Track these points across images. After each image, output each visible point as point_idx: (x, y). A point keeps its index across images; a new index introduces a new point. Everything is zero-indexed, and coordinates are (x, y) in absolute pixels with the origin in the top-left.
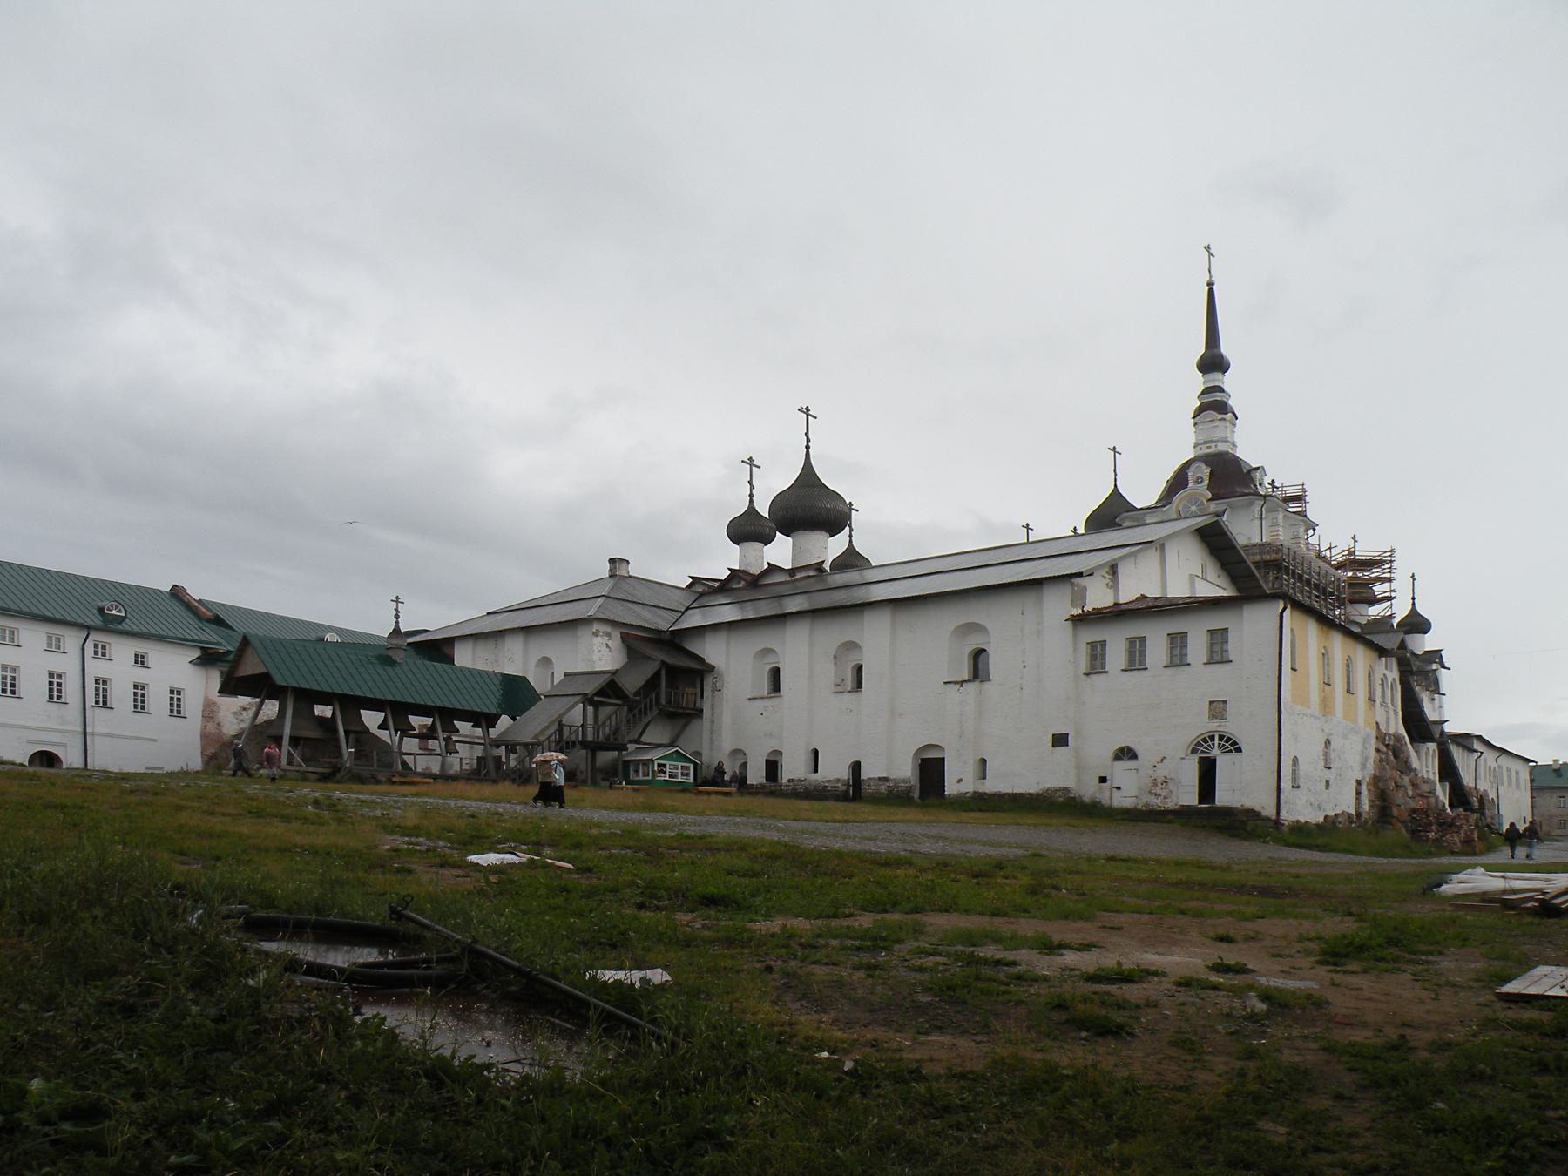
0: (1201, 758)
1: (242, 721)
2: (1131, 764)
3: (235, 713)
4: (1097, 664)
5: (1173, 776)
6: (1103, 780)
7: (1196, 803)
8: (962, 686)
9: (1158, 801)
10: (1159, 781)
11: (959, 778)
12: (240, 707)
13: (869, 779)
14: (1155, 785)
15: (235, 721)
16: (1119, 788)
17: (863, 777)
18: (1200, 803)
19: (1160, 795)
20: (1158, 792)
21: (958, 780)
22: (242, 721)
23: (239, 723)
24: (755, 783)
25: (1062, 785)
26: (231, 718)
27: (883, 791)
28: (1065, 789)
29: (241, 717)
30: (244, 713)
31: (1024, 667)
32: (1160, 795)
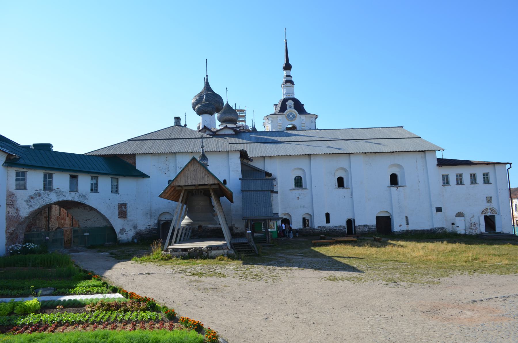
0: (484, 216)
1: (31, 206)
2: (462, 218)
3: (26, 201)
4: (446, 181)
5: (477, 222)
6: (453, 224)
7: (485, 231)
8: (398, 188)
9: (473, 231)
10: (473, 224)
11: (400, 224)
12: (30, 196)
13: (359, 226)
14: (471, 226)
15: (27, 207)
16: (458, 227)
17: (356, 225)
18: (486, 231)
19: (473, 229)
20: (473, 228)
21: (398, 225)
22: (31, 206)
23: (29, 208)
24: (296, 229)
25: (441, 226)
26: (24, 205)
27: (366, 231)
28: (443, 228)
29: (30, 204)
30: (32, 200)
31: (419, 182)
32: (473, 229)
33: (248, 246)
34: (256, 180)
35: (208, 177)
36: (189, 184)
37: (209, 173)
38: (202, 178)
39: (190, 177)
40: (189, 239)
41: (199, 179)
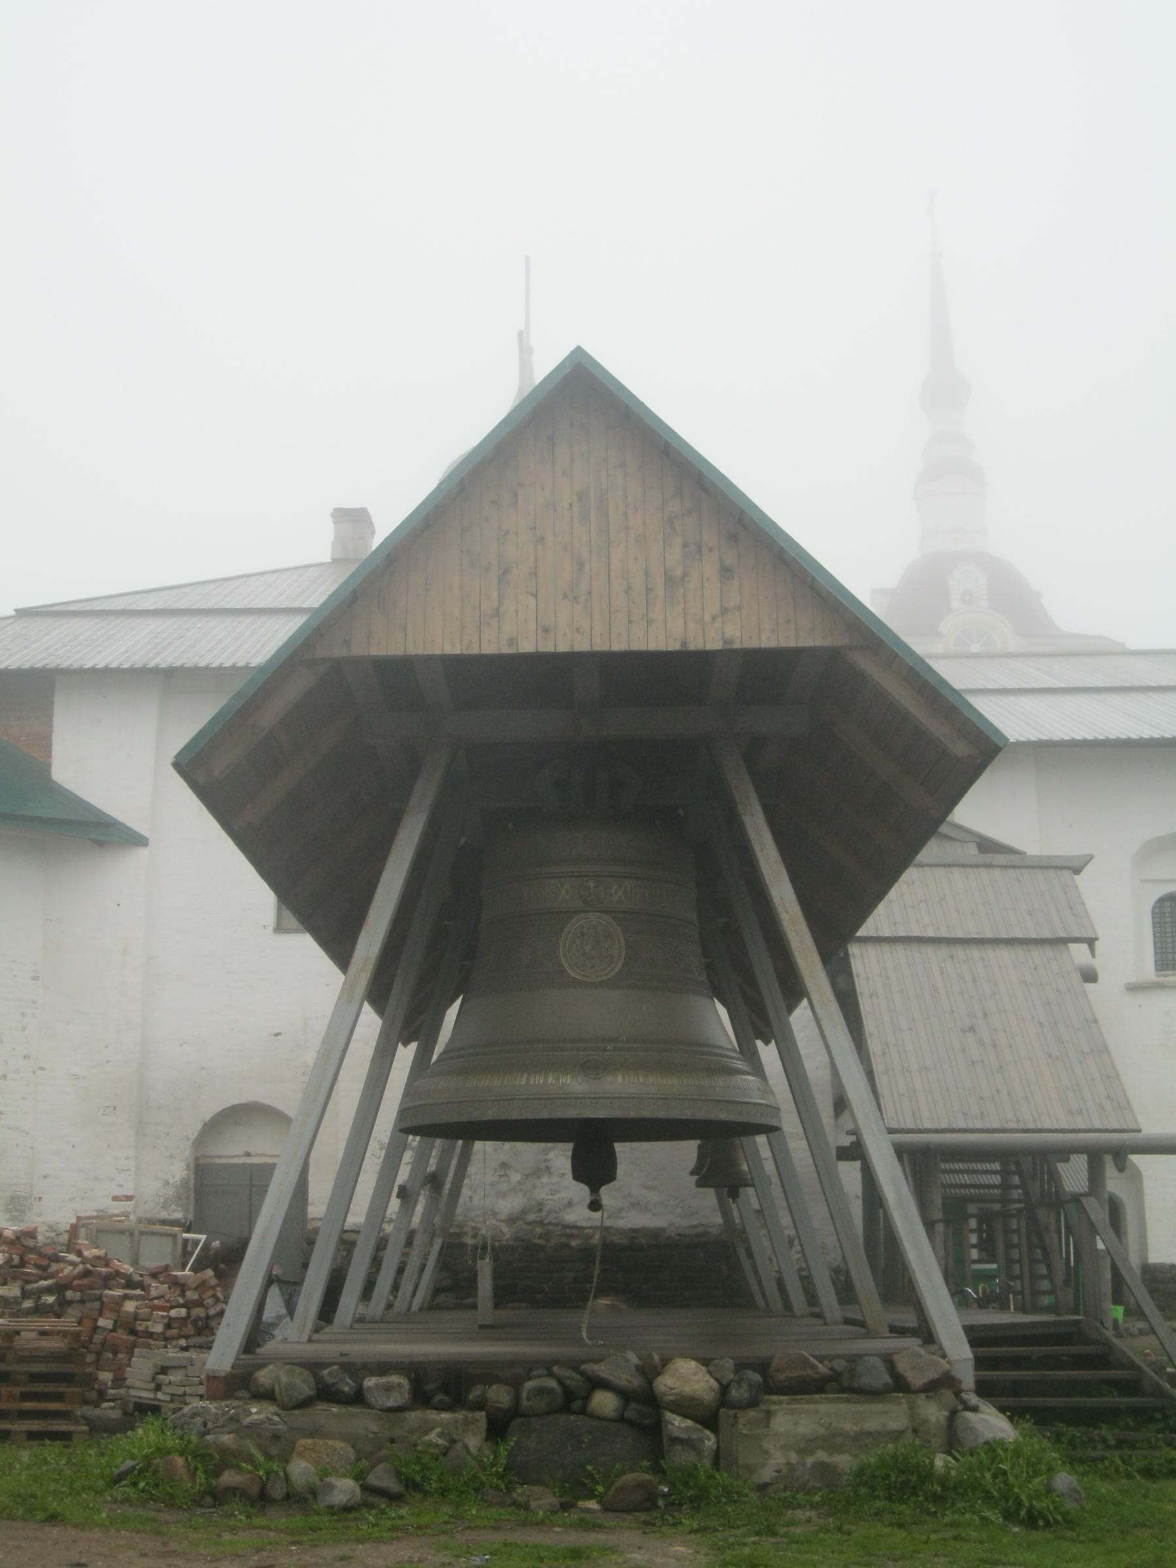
33: (1083, 1362)
34: (941, 872)
35: (726, 572)
36: (511, 642)
37: (734, 538)
38: (660, 590)
39: (534, 574)
40: (421, 1309)
41: (628, 590)
